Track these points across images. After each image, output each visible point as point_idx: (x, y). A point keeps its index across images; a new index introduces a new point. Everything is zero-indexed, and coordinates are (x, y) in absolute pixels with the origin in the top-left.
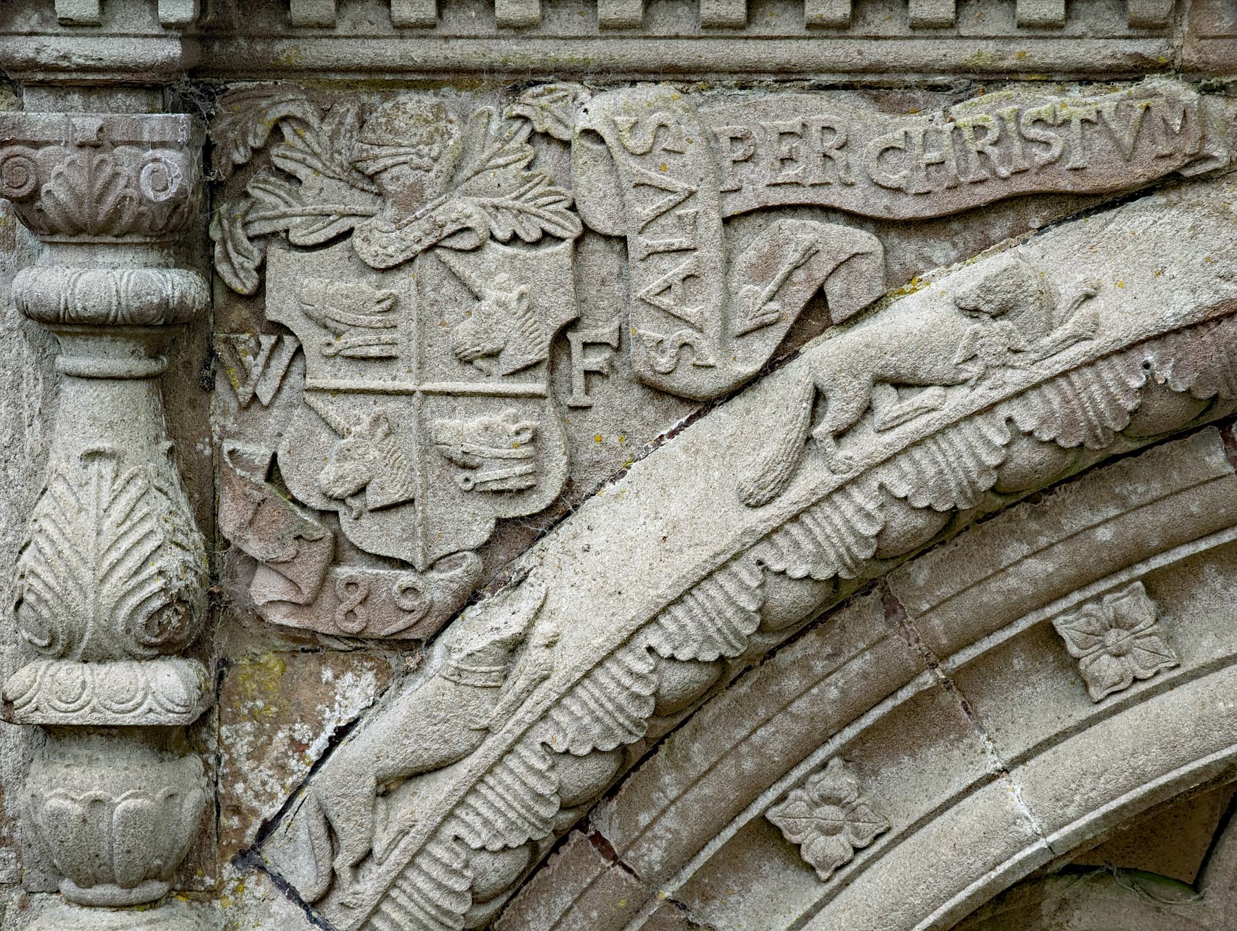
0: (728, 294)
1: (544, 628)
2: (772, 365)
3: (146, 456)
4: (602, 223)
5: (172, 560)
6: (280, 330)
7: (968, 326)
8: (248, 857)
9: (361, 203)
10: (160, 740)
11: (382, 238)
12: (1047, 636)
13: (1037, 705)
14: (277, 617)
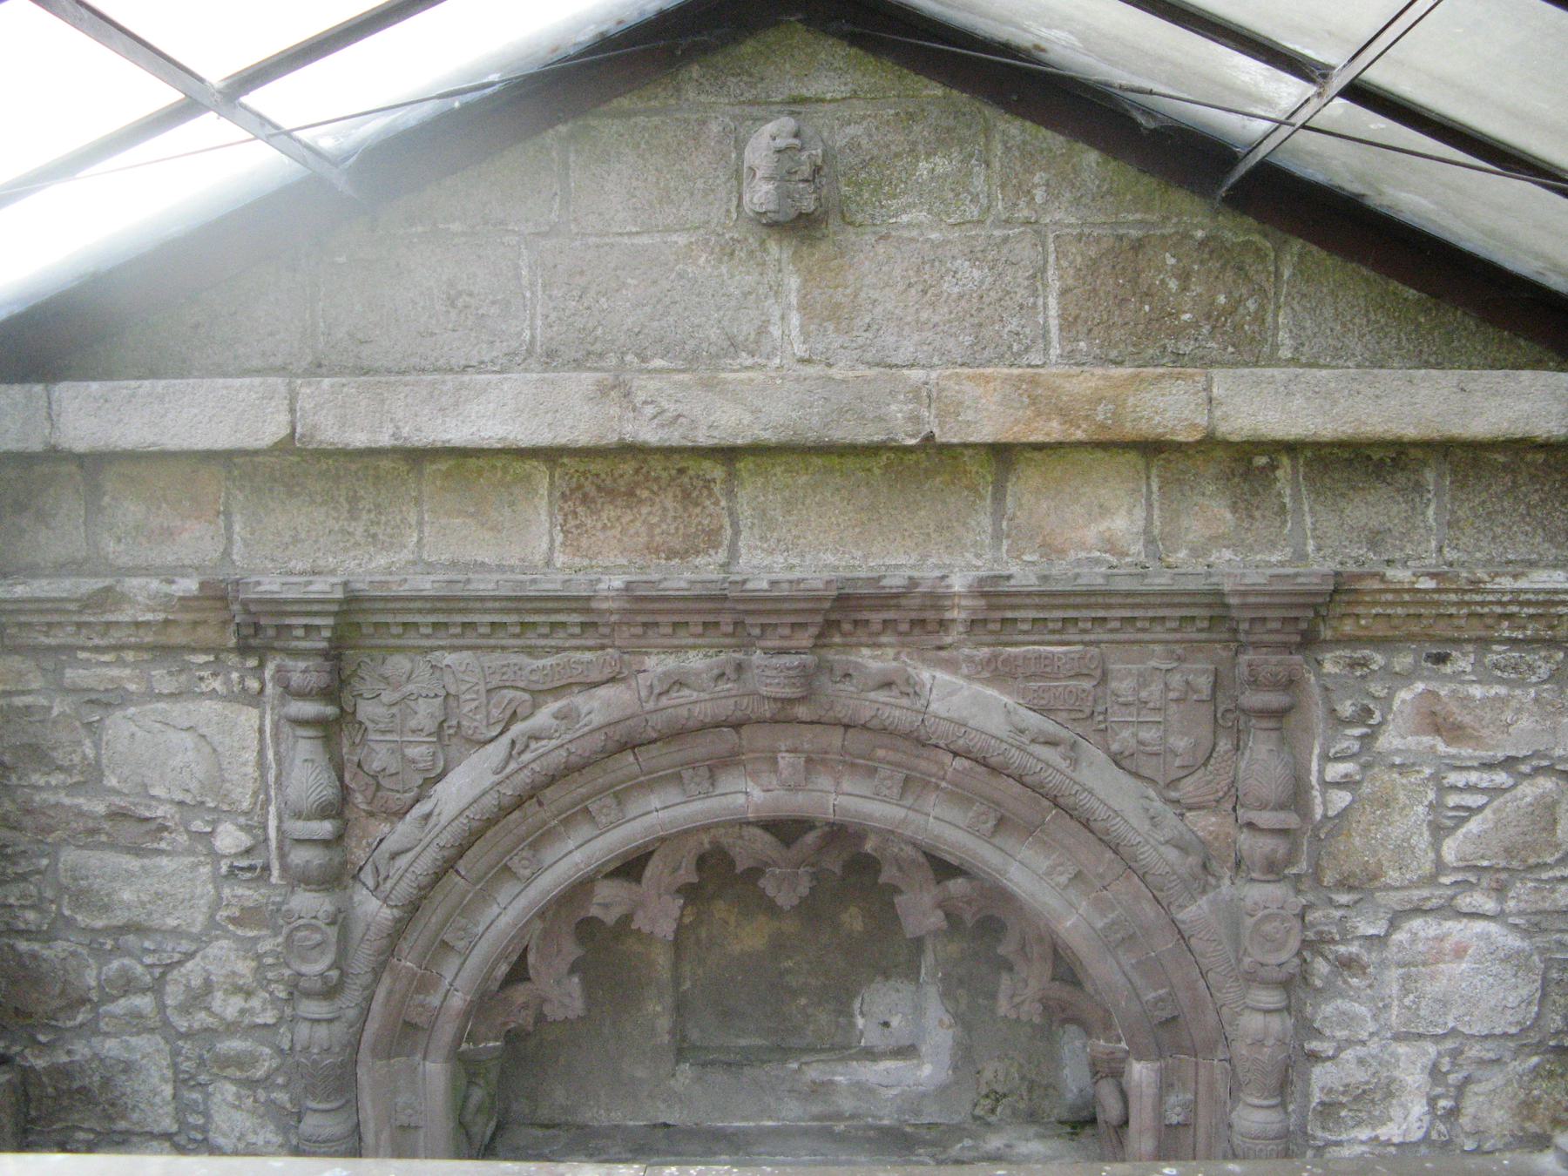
0: (488, 713)
1: (437, 811)
2: (501, 733)
3: (322, 759)
4: (452, 691)
5: (330, 790)
6: (361, 723)
7: (555, 722)
8: (355, 877)
9: (382, 686)
10: (325, 843)
11: (386, 697)
12: (586, 810)
13: (586, 831)
14: (363, 806)
